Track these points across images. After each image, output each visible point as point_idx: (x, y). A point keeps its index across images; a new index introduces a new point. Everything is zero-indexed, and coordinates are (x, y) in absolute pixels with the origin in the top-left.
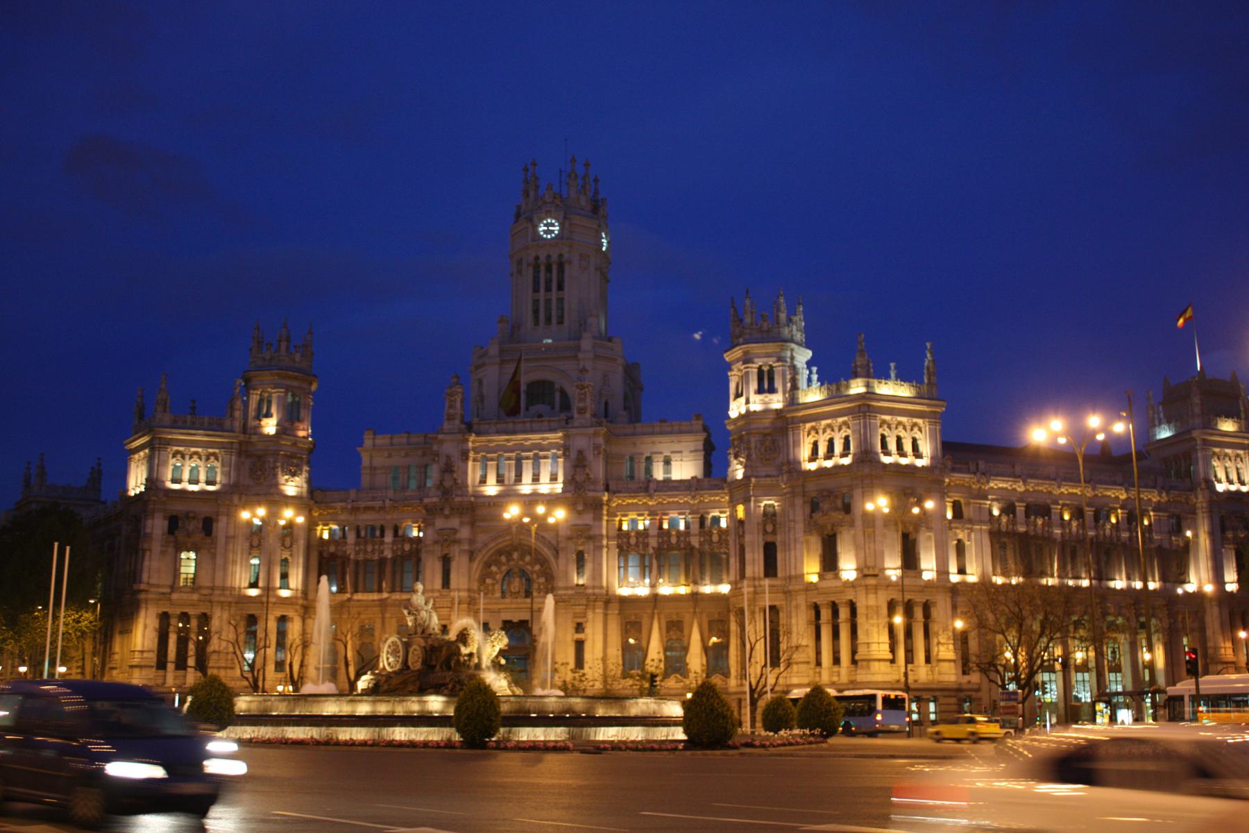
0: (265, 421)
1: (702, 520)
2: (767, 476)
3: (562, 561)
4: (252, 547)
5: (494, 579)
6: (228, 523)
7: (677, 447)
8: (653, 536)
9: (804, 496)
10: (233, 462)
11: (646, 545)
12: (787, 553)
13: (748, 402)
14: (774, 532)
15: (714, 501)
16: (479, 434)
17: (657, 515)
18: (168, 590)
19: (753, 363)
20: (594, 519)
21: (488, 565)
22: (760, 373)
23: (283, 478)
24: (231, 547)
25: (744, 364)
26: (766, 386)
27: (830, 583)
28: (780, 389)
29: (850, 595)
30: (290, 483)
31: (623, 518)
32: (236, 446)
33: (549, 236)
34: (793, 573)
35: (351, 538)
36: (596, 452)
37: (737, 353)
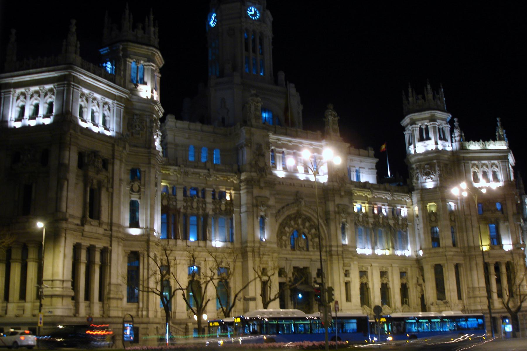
0: (141, 87)
3: (333, 228)
4: (132, 190)
5: (286, 235)
7: (363, 165)
8: (370, 217)
11: (368, 223)
12: (465, 234)
13: (436, 143)
14: (454, 221)
16: (275, 133)
18: (78, 222)
19: (437, 122)
21: (282, 226)
22: (421, 130)
25: (430, 122)
26: (442, 137)
27: (496, 252)
28: (449, 140)
29: (508, 259)
34: (472, 245)
35: (180, 195)
37: (427, 114)
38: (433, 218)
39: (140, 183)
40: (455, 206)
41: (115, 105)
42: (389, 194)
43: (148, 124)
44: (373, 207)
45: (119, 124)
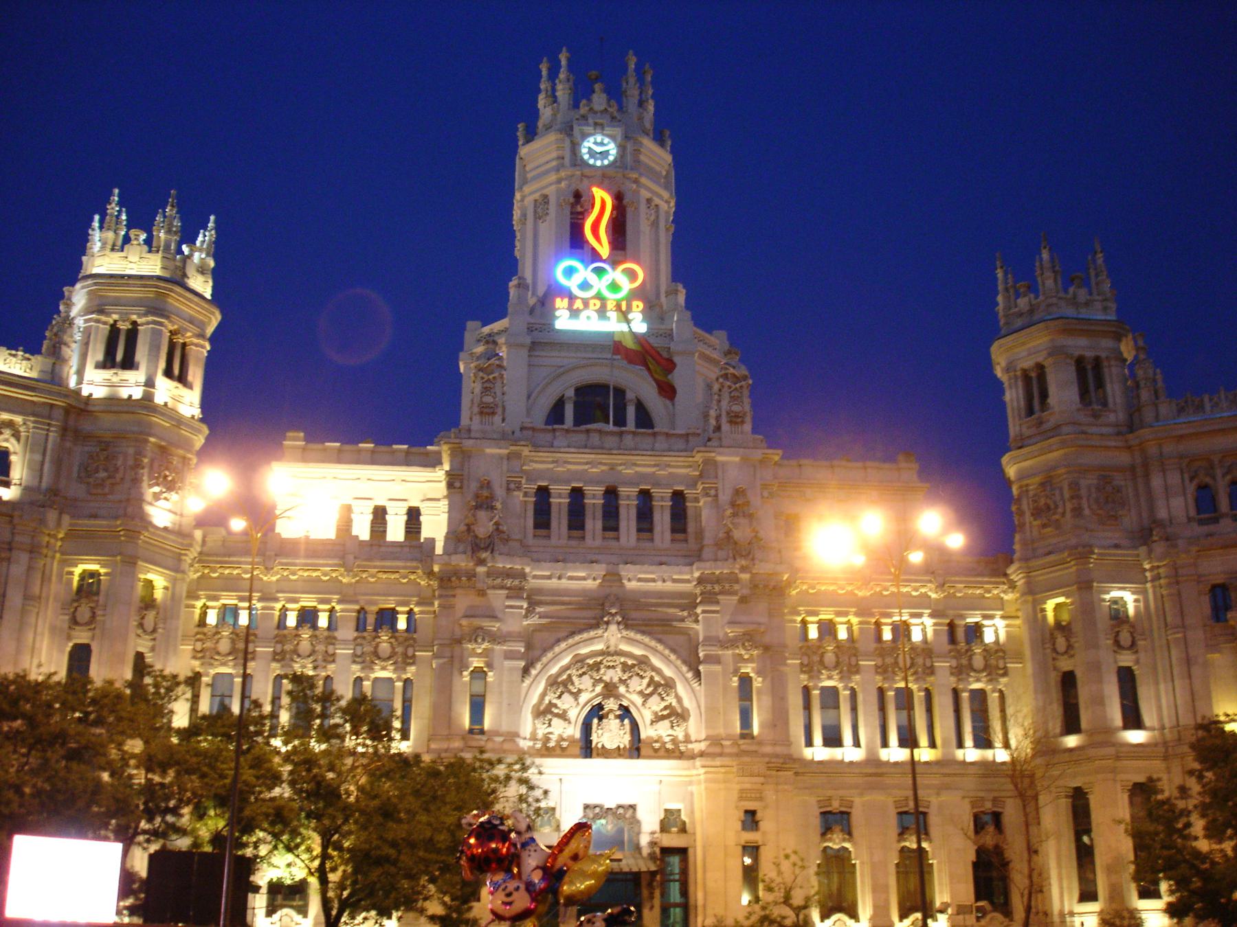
1: (952, 626)
2: (1117, 546)
4: (74, 622)
6: (30, 569)
9: (1198, 582)
10: (50, 446)
14: (1133, 646)
15: (973, 596)
17: (872, 615)
20: (771, 615)
23: (150, 491)
24: (33, 620)
30: (161, 503)
31: (809, 619)
32: (58, 414)
33: (599, 163)
36: (766, 494)
38: (1061, 643)
39: (98, 601)
40: (1136, 601)
41: (32, 425)
42: (930, 581)
43: (131, 462)
44: (878, 625)
45: (38, 467)
